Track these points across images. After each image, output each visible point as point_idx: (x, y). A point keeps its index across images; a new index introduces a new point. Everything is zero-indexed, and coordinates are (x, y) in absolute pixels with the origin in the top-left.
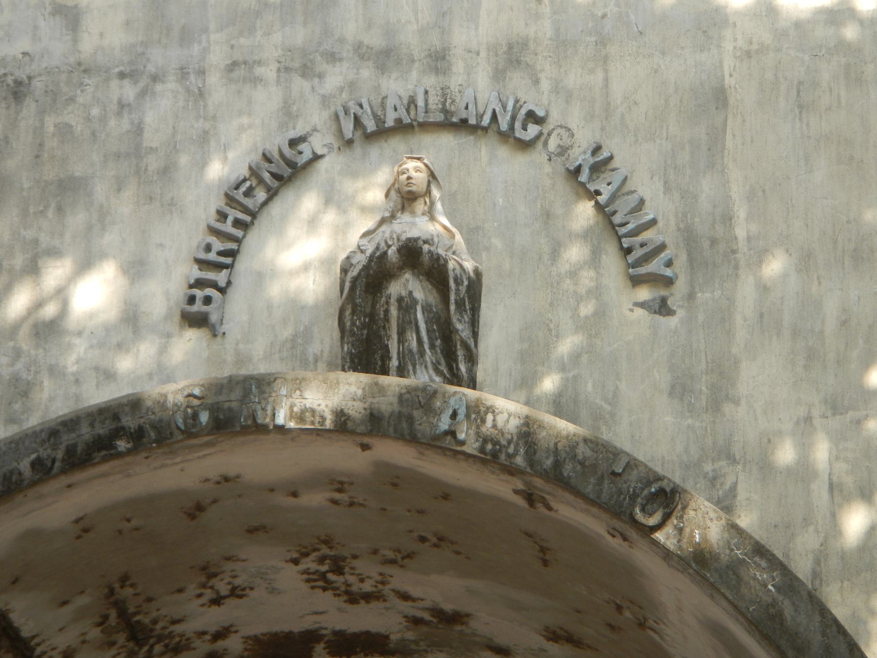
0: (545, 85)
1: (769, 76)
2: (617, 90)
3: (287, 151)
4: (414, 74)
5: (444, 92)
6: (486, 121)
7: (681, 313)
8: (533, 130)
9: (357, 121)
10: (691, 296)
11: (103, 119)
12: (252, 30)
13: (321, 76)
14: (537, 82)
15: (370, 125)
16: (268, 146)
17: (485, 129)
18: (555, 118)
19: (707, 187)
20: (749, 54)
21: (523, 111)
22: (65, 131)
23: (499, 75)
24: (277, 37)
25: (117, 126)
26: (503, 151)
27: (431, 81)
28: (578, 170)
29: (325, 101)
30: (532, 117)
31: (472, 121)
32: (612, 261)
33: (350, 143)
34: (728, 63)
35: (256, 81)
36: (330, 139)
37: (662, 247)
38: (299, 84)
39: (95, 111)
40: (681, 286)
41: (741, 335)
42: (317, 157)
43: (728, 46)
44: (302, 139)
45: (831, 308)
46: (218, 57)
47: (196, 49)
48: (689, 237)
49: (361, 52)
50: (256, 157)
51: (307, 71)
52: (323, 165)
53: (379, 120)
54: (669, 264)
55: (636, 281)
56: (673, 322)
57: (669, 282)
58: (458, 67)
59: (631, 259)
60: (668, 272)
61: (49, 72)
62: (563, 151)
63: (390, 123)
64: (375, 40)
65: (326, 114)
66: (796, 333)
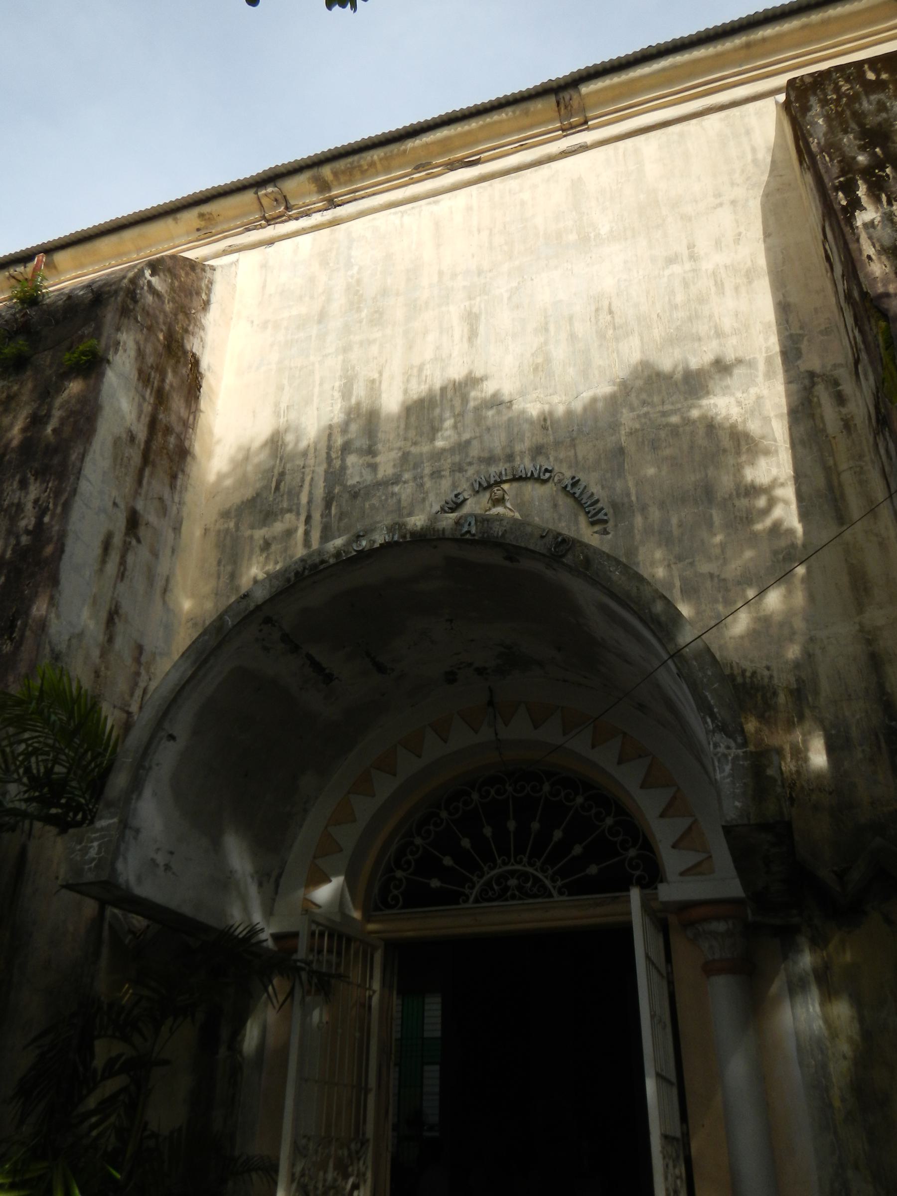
0: (552, 459)
1: (640, 440)
2: (580, 457)
3: (454, 499)
4: (501, 464)
5: (513, 468)
6: (529, 475)
7: (612, 533)
8: (547, 475)
9: (480, 484)
10: (616, 526)
11: (386, 500)
12: (440, 459)
13: (466, 471)
14: (548, 458)
15: (485, 484)
16: (447, 498)
17: (529, 478)
18: (556, 469)
19: (619, 485)
20: (631, 433)
21: (543, 469)
22: (372, 507)
23: (533, 459)
24: (449, 461)
25: (392, 502)
26: (537, 486)
27: (507, 465)
28: (566, 486)
29: (468, 479)
30: (547, 470)
31: (524, 476)
32: (583, 520)
33: (478, 492)
34: (623, 438)
35: (441, 477)
36: (470, 492)
37: (602, 509)
38: (457, 475)
39: (383, 498)
40: (611, 524)
41: (638, 537)
42: (465, 500)
43: (623, 432)
44: (459, 494)
45: (674, 521)
46: (427, 471)
47: (419, 470)
48: (614, 505)
49: (481, 460)
50: (443, 503)
51: (461, 470)
52: (468, 502)
53: (488, 482)
54: (606, 514)
55: (593, 524)
56: (610, 536)
57: (606, 522)
58: (518, 458)
59: (589, 515)
60: (605, 518)
61: (366, 487)
62: (560, 481)
63: (492, 482)
64: (486, 455)
65: (468, 484)
66: (660, 533)
